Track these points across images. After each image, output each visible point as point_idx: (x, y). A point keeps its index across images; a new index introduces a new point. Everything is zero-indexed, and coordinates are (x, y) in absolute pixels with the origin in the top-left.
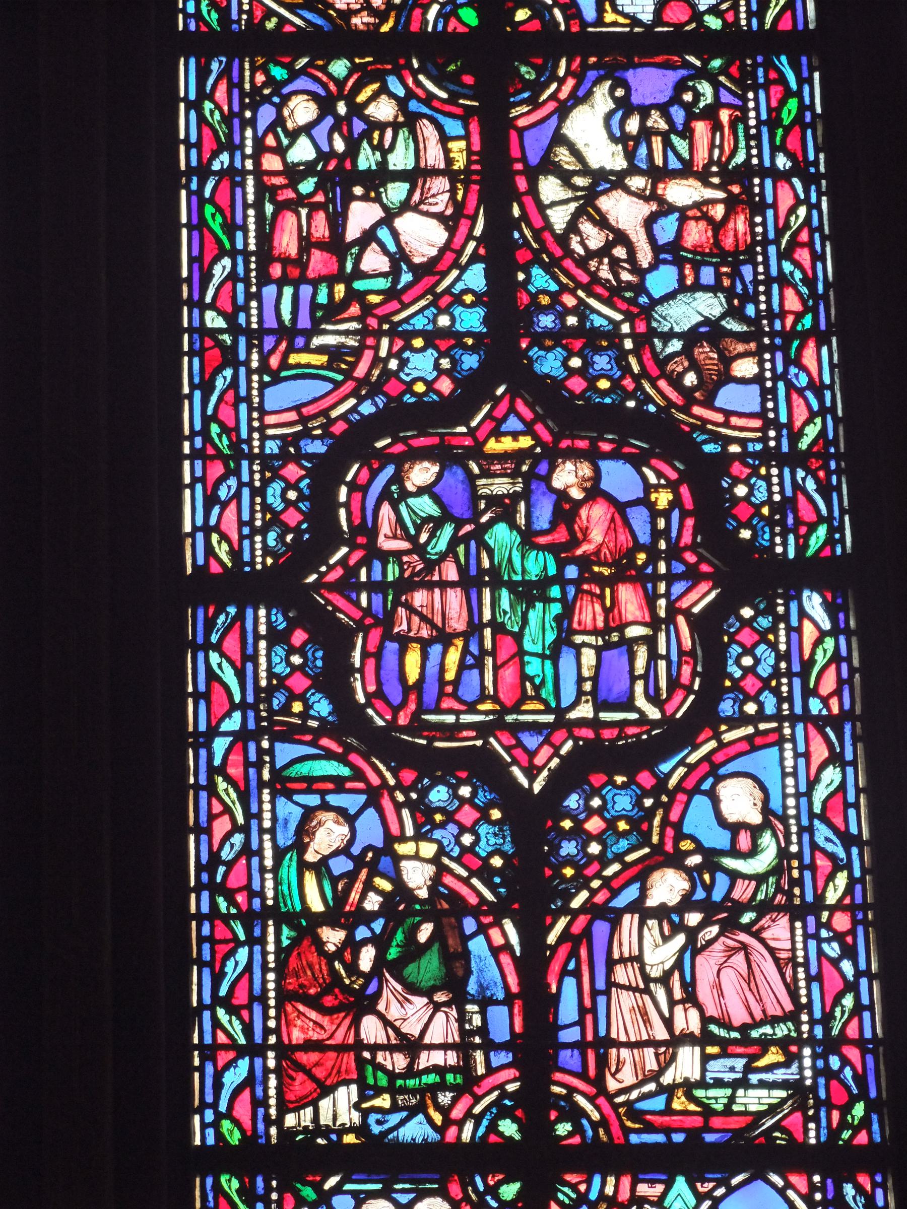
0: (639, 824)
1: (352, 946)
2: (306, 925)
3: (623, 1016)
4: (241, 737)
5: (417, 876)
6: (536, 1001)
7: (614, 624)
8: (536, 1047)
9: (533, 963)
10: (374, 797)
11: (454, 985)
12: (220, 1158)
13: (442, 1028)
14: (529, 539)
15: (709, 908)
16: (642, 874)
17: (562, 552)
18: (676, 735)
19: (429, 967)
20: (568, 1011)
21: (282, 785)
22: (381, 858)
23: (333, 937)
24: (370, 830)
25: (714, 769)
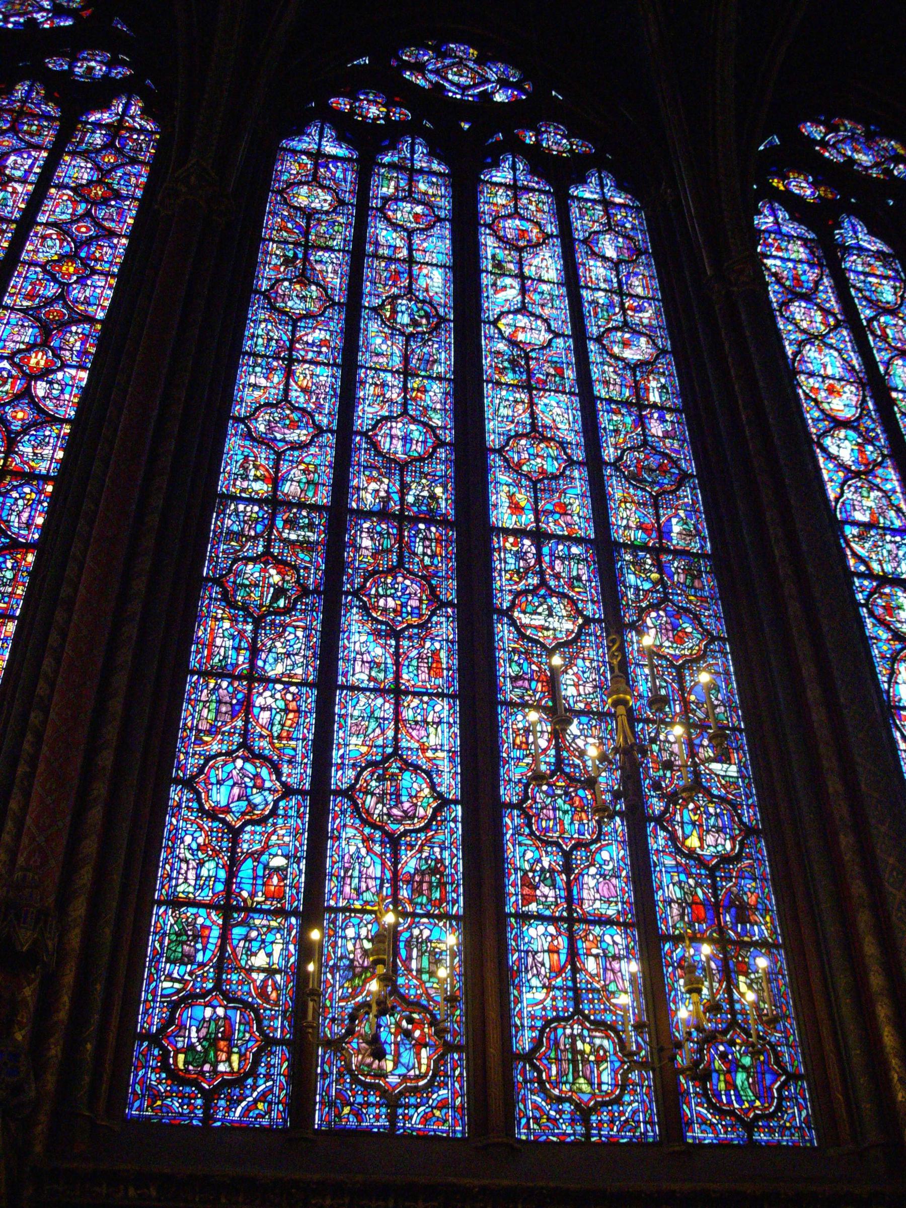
0: (587, 858)
1: (534, 877)
2: (526, 873)
3: (585, 894)
4: (512, 835)
5: (546, 865)
6: (569, 890)
7: (581, 819)
8: (569, 899)
9: (569, 883)
10: (537, 848)
11: (554, 886)
12: (511, 915)
13: (552, 893)
14: (565, 802)
15: (601, 876)
16: (588, 867)
17: (571, 805)
18: (594, 842)
19: (549, 882)
20: (575, 892)
21: (520, 844)
22: (539, 861)
23: (530, 875)
24: (537, 855)
25: (600, 849)
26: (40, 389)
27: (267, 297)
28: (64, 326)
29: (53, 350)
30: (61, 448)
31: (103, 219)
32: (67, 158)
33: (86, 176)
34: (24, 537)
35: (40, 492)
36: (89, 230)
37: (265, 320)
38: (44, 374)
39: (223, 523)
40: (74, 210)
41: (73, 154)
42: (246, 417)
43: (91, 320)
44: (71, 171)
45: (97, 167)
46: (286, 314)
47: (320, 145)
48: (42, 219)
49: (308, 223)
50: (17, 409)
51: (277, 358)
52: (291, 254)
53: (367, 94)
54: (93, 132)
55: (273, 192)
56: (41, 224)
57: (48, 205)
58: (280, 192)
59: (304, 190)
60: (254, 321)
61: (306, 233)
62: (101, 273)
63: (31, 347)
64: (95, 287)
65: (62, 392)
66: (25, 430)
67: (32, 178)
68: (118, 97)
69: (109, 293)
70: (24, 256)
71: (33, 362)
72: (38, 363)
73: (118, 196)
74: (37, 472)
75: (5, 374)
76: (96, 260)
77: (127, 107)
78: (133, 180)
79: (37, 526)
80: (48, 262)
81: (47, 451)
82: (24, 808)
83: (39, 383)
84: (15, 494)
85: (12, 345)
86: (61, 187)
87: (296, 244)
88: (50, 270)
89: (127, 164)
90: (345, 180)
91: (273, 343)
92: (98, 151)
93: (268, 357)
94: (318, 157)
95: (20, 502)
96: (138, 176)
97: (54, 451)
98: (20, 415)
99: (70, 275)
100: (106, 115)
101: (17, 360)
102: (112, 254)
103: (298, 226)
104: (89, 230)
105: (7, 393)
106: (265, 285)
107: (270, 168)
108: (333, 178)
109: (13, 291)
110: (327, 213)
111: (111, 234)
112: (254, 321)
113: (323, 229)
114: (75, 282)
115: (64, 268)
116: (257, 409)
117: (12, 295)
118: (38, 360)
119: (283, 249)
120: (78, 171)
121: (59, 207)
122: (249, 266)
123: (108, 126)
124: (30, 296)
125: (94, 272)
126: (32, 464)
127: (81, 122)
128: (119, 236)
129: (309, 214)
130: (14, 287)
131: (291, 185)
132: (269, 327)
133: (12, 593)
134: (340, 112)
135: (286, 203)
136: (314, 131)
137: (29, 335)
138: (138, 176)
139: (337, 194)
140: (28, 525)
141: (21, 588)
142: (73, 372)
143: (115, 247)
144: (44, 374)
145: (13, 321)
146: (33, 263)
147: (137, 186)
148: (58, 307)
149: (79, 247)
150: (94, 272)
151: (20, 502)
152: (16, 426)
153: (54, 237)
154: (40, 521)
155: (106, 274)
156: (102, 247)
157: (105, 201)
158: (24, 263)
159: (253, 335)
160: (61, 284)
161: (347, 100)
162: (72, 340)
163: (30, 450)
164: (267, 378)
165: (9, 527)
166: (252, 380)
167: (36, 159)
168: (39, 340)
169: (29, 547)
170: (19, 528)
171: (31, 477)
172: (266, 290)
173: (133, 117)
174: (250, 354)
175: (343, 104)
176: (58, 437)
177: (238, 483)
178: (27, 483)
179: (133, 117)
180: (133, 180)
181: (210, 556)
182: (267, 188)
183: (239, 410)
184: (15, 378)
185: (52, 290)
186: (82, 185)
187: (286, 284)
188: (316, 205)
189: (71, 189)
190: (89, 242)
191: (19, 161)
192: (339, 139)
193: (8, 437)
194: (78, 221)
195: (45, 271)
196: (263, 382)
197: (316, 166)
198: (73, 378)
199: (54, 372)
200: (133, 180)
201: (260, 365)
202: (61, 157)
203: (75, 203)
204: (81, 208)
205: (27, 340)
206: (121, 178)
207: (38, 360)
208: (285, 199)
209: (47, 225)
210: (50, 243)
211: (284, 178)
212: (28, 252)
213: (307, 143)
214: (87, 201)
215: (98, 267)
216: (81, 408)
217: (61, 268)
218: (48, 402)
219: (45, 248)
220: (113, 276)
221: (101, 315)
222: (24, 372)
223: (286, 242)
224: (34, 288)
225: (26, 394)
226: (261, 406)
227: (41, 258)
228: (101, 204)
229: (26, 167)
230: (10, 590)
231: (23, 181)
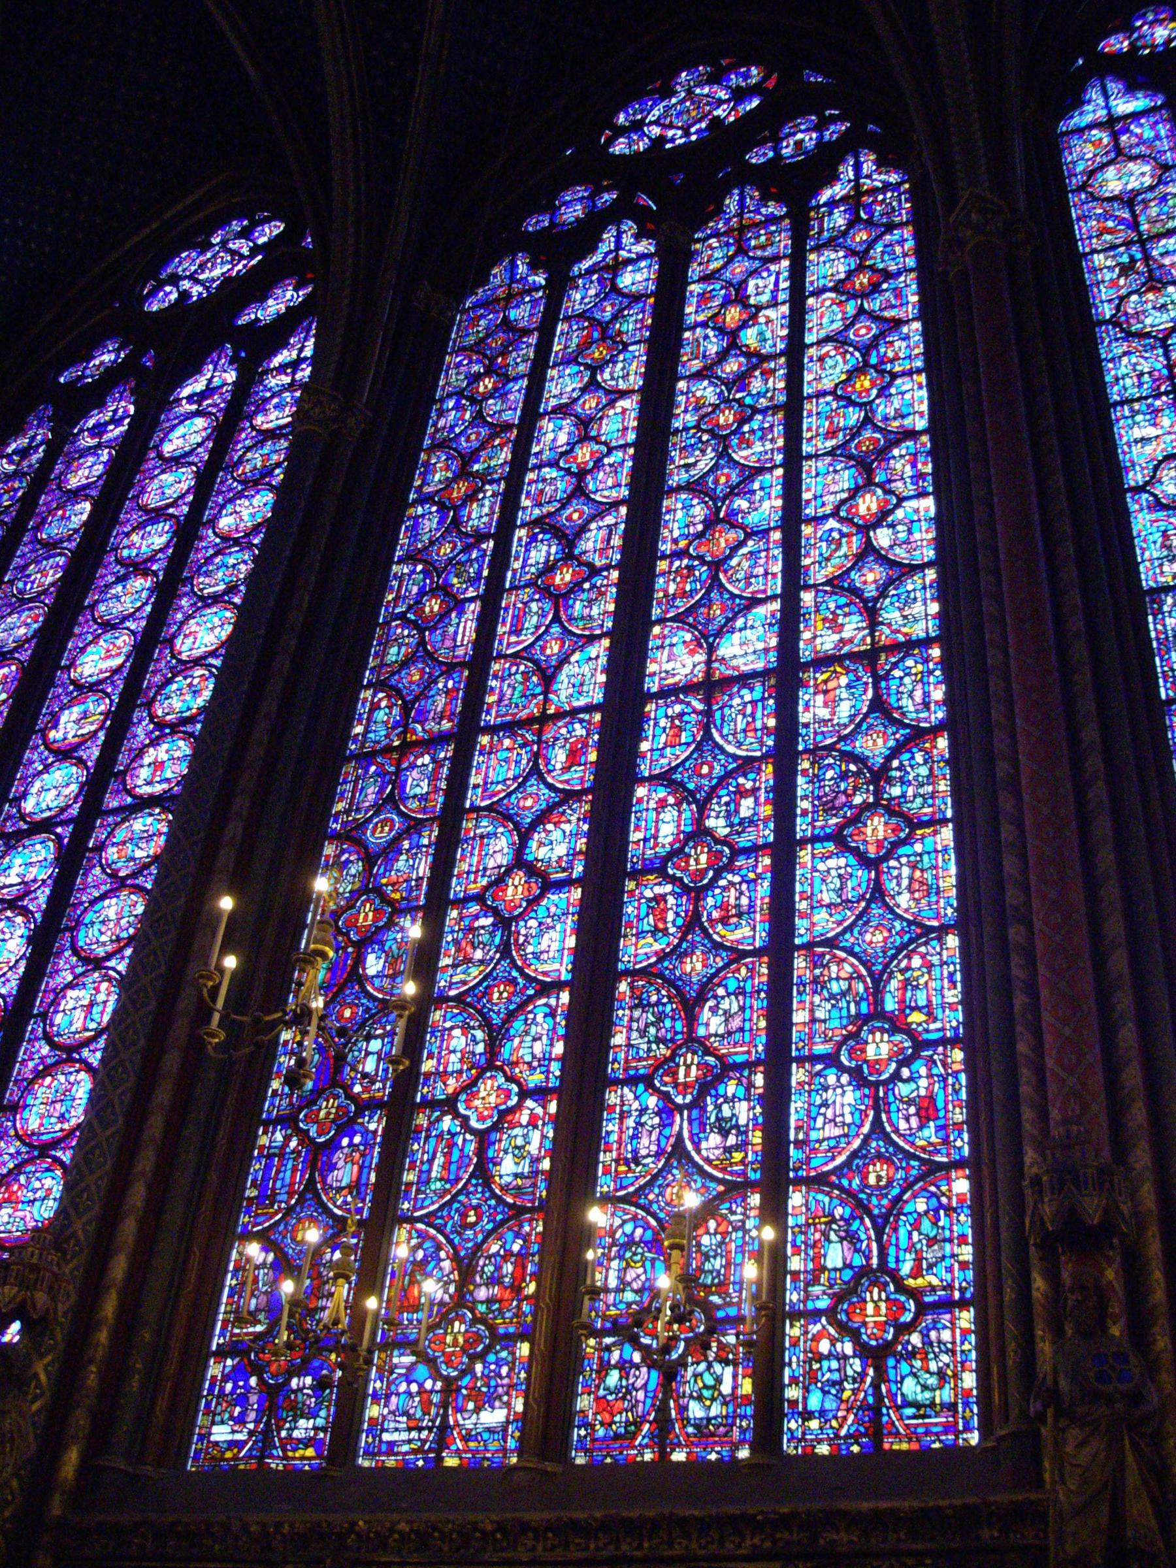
26: (882, 537)
27: (1117, 324)
28: (882, 454)
29: (881, 485)
30: (933, 600)
31: (881, 310)
32: (812, 257)
33: (842, 269)
34: (926, 720)
35: (926, 661)
36: (869, 329)
37: (1125, 354)
38: (881, 518)
39: (1164, 626)
40: (844, 313)
41: (818, 249)
42: (1147, 483)
43: (912, 434)
44: (823, 270)
45: (851, 253)
46: (1148, 335)
47: (1107, 107)
48: (810, 338)
49: (1133, 212)
50: (865, 571)
51: (1158, 396)
52: (1125, 259)
53: (1143, 16)
54: (830, 214)
55: (1073, 191)
56: (812, 345)
57: (812, 320)
58: (1082, 188)
59: (1111, 172)
60: (1112, 360)
61: (1134, 225)
62: (904, 374)
63: (854, 493)
64: (903, 394)
65: (910, 532)
66: (883, 593)
67: (782, 296)
68: (843, 160)
69: (924, 393)
70: (807, 390)
71: (862, 510)
72: (869, 509)
73: (888, 275)
74: (914, 637)
75: (836, 535)
76: (892, 361)
77: (858, 167)
78: (898, 250)
79: (936, 702)
80: (837, 385)
81: (918, 608)
82: (1039, 1047)
83: (878, 531)
84: (897, 673)
85: (831, 498)
86: (818, 293)
87: (1128, 244)
88: (843, 395)
89: (883, 234)
90: (1157, 137)
91: (1146, 378)
92: (844, 234)
93: (1146, 398)
94: (1113, 124)
95: (907, 680)
96: (902, 242)
97: (925, 604)
98: (870, 577)
99: (868, 391)
100: (837, 188)
101: (843, 514)
102: (908, 346)
103: (1122, 221)
104: (869, 329)
105: (846, 556)
106: (1108, 311)
107: (1057, 163)
108: (1141, 141)
109: (809, 435)
110: (1151, 188)
111: (897, 323)
112: (1112, 360)
113: (1154, 211)
114: (878, 396)
115: (858, 386)
116: (1156, 468)
117: (809, 440)
118: (868, 504)
119: (1114, 257)
120: (828, 266)
121: (825, 316)
122: (1078, 293)
123: (844, 199)
124: (831, 434)
125: (894, 376)
126: (904, 630)
127: (813, 208)
128: (907, 322)
129: (1129, 199)
130: (809, 429)
131: (1092, 173)
132: (1134, 360)
133: (934, 792)
134: (1118, 56)
135: (1095, 199)
136: (1094, 94)
137: (846, 479)
138: (902, 242)
139: (1155, 159)
140: (926, 705)
141: (942, 782)
142: (914, 503)
143: (907, 338)
144: (881, 518)
145: (822, 470)
146: (821, 394)
147: (905, 255)
148: (868, 433)
149: (866, 354)
150: (894, 376)
151: (907, 680)
152: (871, 591)
153: (833, 353)
154: (938, 694)
155: (909, 373)
156: (892, 343)
157: (875, 288)
158: (810, 397)
159: (1117, 379)
160: (861, 405)
161: (1121, 37)
162: (899, 466)
163: (897, 614)
164: (1155, 425)
165: (903, 714)
166: (1137, 433)
167: (778, 274)
168: (860, 481)
169: (935, 731)
170: (917, 712)
171: (909, 646)
172: (1113, 316)
173: (869, 177)
174: (1122, 403)
175: (1118, 44)
176: (924, 588)
177: (1166, 568)
178: (907, 655)
179: (869, 177)
180: (898, 249)
181: (1164, 672)
182: (1063, 191)
183: (1135, 478)
184: (849, 535)
185: (853, 416)
186: (841, 281)
187: (1134, 298)
188: (1134, 184)
189: (831, 290)
190: (873, 344)
191: (761, 283)
192: (1130, 90)
193: (866, 608)
194: (853, 324)
195: (838, 398)
196: (1152, 432)
197: (1115, 136)
198: (917, 511)
199: (892, 511)
200: (898, 249)
201: (1138, 412)
202: (805, 259)
203: (840, 304)
204: (851, 308)
205: (846, 486)
206: (883, 253)
207: (868, 504)
208: (1091, 194)
209: (820, 343)
210: (829, 362)
211: (1079, 169)
212: (809, 383)
213: (1092, 111)
214: (854, 297)
215: (897, 369)
216: (940, 543)
217: (853, 386)
218: (897, 550)
219: (826, 371)
220: (919, 371)
221: (921, 424)
222: (856, 525)
223: (1113, 247)
224: (832, 423)
225: (869, 550)
226: (1160, 462)
227: (827, 384)
228: (872, 292)
229: (771, 287)
230: (930, 789)
231: (774, 303)
